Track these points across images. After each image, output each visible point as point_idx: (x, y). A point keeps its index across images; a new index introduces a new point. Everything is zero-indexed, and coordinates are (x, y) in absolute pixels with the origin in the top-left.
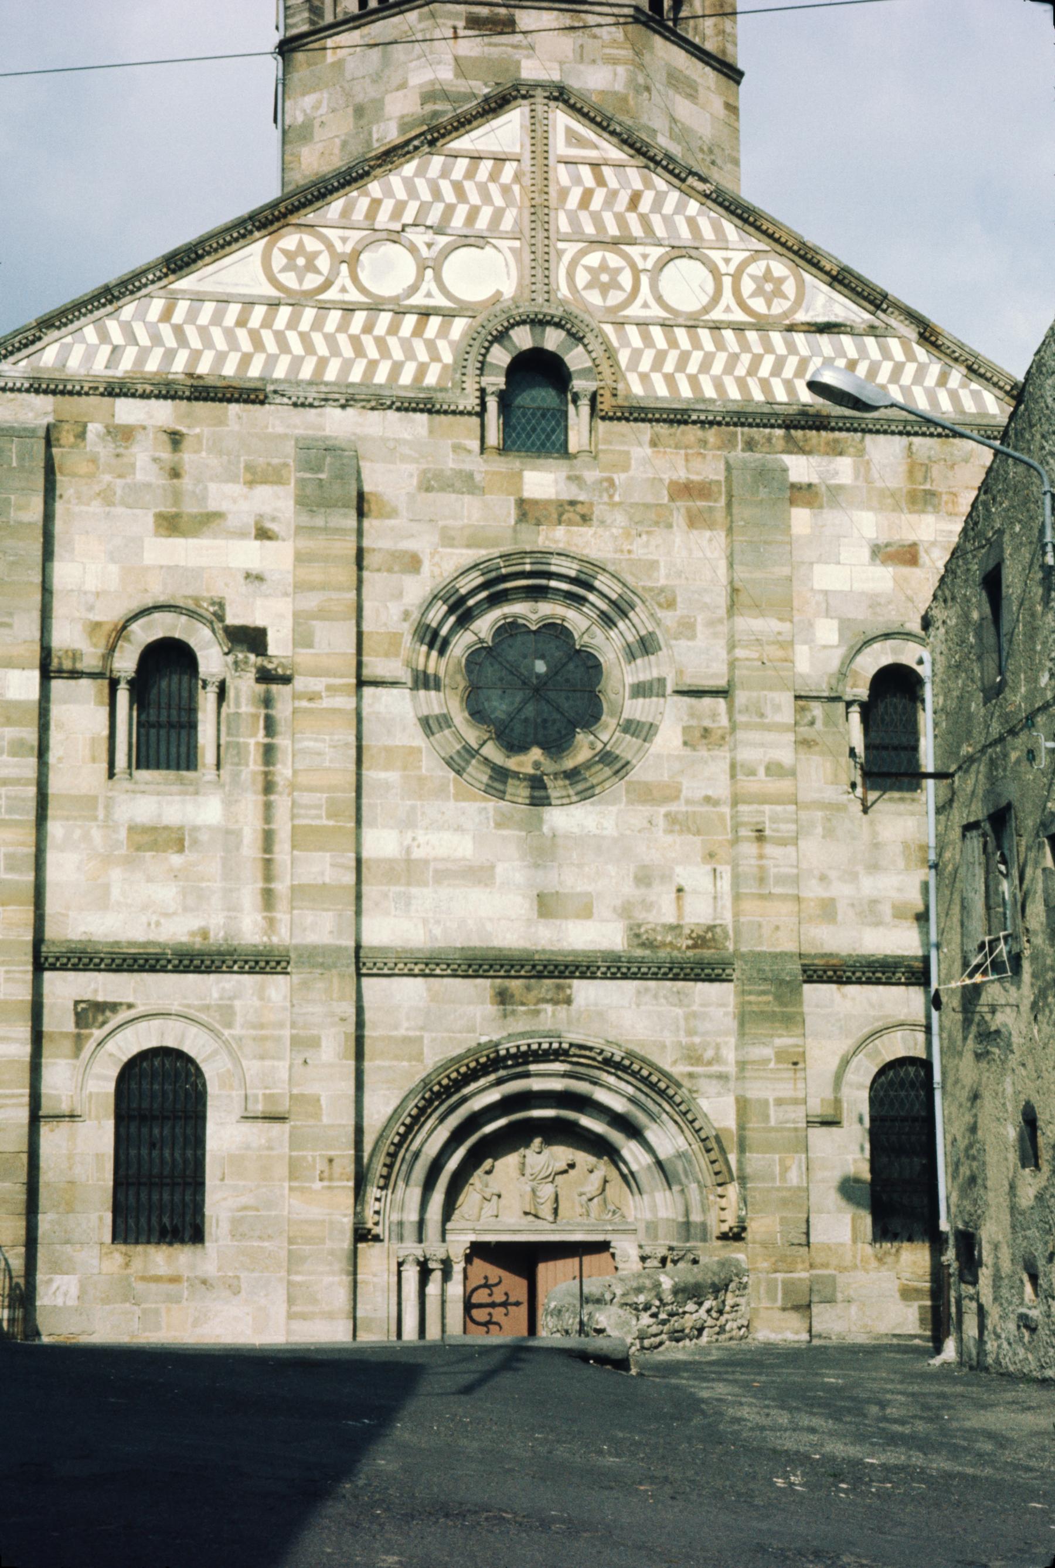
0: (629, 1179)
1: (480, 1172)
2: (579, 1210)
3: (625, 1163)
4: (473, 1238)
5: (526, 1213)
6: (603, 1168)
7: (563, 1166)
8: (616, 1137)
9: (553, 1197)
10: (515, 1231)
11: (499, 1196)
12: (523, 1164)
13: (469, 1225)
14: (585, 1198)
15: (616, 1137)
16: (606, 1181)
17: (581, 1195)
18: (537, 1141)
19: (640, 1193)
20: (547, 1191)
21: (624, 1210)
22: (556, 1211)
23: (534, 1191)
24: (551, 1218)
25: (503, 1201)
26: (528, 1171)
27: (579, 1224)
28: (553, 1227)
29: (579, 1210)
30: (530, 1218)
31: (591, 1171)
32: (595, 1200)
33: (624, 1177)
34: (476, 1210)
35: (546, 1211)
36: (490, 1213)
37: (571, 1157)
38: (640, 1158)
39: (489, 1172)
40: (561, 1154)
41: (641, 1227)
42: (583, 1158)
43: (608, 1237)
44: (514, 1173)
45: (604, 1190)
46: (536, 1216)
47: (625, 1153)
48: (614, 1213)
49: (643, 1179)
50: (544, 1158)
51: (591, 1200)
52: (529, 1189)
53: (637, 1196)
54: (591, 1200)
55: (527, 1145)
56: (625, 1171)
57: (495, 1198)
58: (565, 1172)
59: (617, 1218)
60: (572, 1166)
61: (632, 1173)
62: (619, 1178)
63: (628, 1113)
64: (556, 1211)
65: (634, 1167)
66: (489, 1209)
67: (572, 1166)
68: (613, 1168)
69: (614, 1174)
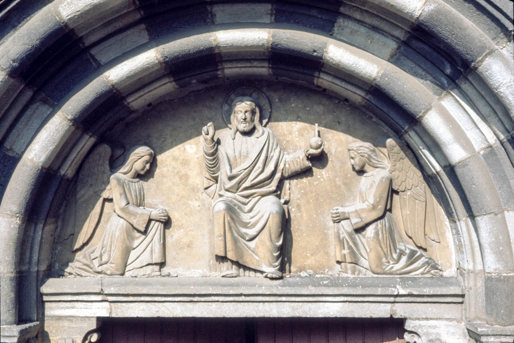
0: (448, 186)
1: (122, 174)
2: (336, 252)
3: (435, 146)
4: (103, 310)
5: (222, 259)
6: (387, 163)
7: (295, 159)
8: (410, 86)
9: (274, 224)
10: (191, 297)
11: (167, 223)
12: (214, 154)
13: (91, 282)
14: (346, 226)
15: (410, 86)
16: (393, 192)
17: (338, 219)
18: (243, 107)
19: (472, 216)
20: (265, 209)
21: (436, 253)
22: (284, 254)
23: (231, 210)
24: (271, 270)
25: (174, 235)
26: (224, 171)
27: (335, 282)
28: (276, 287)
29: (336, 252)
30: (227, 269)
31: (361, 172)
32: (370, 231)
33: (430, 179)
34: (116, 254)
35: (261, 253)
36: (145, 258)
37: (315, 140)
38: (472, 134)
39: (145, 175)
40: (296, 136)
41: (475, 289)
42: (342, 145)
43: (400, 311)
44: (198, 177)
45: (388, 210)
46: (238, 265)
47: (433, 121)
48: (412, 258)
49: (479, 181)
50: (250, 141)
51: (360, 230)
52: (221, 206)
53: (464, 223)
54: (360, 230)
55: (224, 122)
56: (435, 165)
57: (156, 228)
58: (306, 172)
59: (418, 269)
60: (319, 159)
61: (451, 170)
62: (422, 187)
63: (438, 12)
64: (284, 254)
65: (456, 153)
66: (145, 250)
67: (319, 159)
68: (407, 163)
69: (411, 178)
